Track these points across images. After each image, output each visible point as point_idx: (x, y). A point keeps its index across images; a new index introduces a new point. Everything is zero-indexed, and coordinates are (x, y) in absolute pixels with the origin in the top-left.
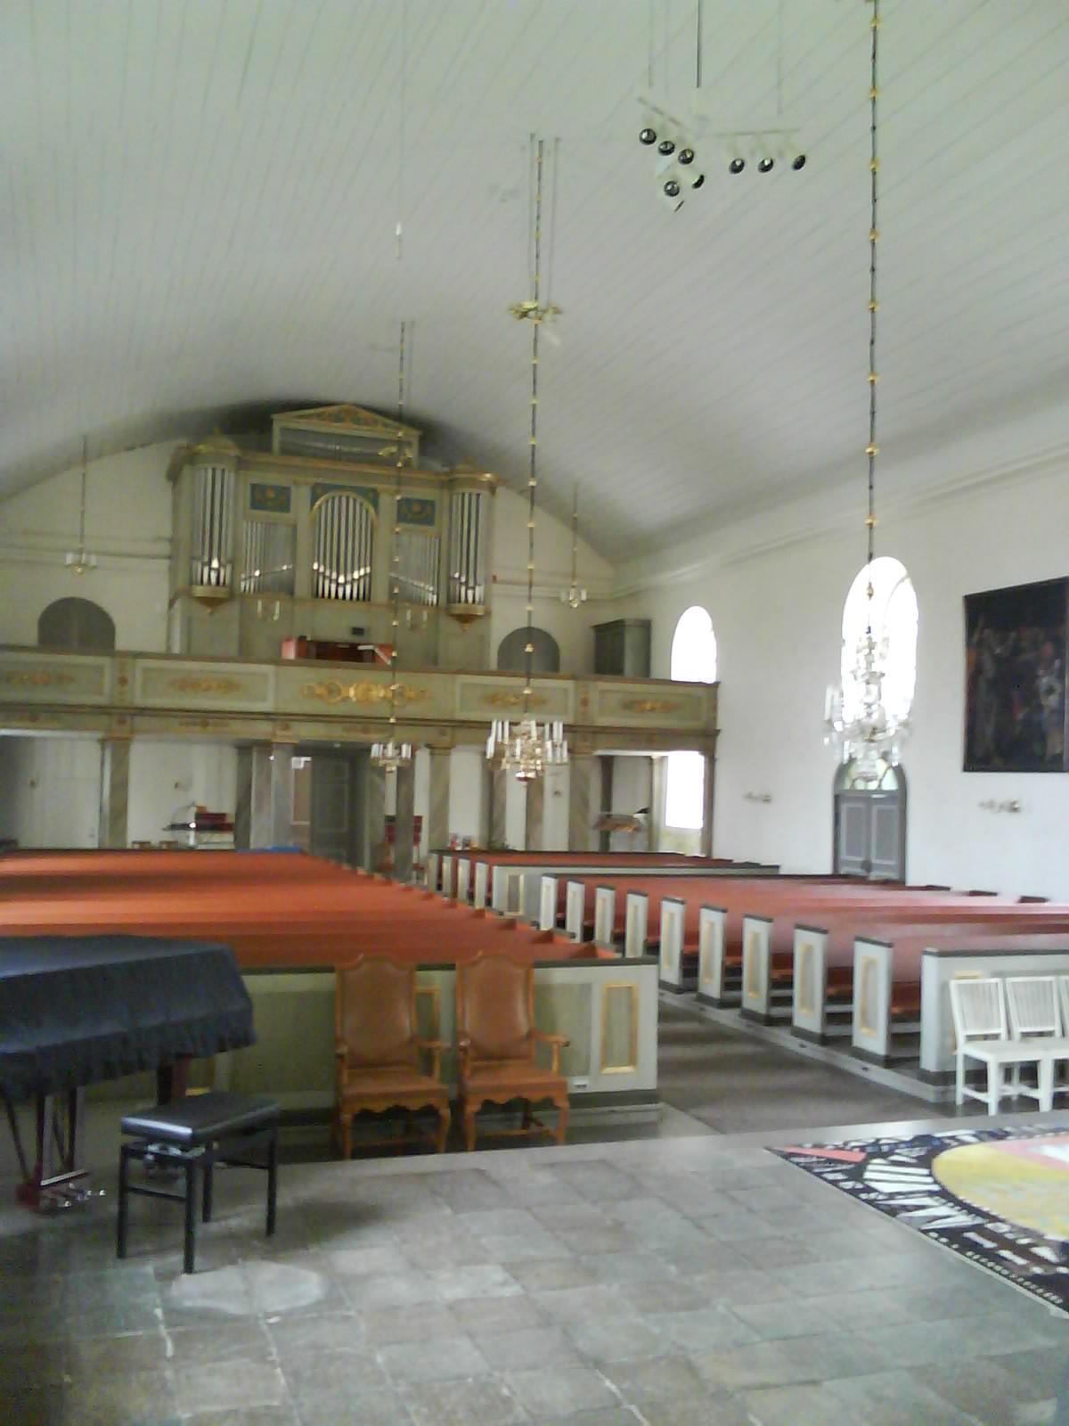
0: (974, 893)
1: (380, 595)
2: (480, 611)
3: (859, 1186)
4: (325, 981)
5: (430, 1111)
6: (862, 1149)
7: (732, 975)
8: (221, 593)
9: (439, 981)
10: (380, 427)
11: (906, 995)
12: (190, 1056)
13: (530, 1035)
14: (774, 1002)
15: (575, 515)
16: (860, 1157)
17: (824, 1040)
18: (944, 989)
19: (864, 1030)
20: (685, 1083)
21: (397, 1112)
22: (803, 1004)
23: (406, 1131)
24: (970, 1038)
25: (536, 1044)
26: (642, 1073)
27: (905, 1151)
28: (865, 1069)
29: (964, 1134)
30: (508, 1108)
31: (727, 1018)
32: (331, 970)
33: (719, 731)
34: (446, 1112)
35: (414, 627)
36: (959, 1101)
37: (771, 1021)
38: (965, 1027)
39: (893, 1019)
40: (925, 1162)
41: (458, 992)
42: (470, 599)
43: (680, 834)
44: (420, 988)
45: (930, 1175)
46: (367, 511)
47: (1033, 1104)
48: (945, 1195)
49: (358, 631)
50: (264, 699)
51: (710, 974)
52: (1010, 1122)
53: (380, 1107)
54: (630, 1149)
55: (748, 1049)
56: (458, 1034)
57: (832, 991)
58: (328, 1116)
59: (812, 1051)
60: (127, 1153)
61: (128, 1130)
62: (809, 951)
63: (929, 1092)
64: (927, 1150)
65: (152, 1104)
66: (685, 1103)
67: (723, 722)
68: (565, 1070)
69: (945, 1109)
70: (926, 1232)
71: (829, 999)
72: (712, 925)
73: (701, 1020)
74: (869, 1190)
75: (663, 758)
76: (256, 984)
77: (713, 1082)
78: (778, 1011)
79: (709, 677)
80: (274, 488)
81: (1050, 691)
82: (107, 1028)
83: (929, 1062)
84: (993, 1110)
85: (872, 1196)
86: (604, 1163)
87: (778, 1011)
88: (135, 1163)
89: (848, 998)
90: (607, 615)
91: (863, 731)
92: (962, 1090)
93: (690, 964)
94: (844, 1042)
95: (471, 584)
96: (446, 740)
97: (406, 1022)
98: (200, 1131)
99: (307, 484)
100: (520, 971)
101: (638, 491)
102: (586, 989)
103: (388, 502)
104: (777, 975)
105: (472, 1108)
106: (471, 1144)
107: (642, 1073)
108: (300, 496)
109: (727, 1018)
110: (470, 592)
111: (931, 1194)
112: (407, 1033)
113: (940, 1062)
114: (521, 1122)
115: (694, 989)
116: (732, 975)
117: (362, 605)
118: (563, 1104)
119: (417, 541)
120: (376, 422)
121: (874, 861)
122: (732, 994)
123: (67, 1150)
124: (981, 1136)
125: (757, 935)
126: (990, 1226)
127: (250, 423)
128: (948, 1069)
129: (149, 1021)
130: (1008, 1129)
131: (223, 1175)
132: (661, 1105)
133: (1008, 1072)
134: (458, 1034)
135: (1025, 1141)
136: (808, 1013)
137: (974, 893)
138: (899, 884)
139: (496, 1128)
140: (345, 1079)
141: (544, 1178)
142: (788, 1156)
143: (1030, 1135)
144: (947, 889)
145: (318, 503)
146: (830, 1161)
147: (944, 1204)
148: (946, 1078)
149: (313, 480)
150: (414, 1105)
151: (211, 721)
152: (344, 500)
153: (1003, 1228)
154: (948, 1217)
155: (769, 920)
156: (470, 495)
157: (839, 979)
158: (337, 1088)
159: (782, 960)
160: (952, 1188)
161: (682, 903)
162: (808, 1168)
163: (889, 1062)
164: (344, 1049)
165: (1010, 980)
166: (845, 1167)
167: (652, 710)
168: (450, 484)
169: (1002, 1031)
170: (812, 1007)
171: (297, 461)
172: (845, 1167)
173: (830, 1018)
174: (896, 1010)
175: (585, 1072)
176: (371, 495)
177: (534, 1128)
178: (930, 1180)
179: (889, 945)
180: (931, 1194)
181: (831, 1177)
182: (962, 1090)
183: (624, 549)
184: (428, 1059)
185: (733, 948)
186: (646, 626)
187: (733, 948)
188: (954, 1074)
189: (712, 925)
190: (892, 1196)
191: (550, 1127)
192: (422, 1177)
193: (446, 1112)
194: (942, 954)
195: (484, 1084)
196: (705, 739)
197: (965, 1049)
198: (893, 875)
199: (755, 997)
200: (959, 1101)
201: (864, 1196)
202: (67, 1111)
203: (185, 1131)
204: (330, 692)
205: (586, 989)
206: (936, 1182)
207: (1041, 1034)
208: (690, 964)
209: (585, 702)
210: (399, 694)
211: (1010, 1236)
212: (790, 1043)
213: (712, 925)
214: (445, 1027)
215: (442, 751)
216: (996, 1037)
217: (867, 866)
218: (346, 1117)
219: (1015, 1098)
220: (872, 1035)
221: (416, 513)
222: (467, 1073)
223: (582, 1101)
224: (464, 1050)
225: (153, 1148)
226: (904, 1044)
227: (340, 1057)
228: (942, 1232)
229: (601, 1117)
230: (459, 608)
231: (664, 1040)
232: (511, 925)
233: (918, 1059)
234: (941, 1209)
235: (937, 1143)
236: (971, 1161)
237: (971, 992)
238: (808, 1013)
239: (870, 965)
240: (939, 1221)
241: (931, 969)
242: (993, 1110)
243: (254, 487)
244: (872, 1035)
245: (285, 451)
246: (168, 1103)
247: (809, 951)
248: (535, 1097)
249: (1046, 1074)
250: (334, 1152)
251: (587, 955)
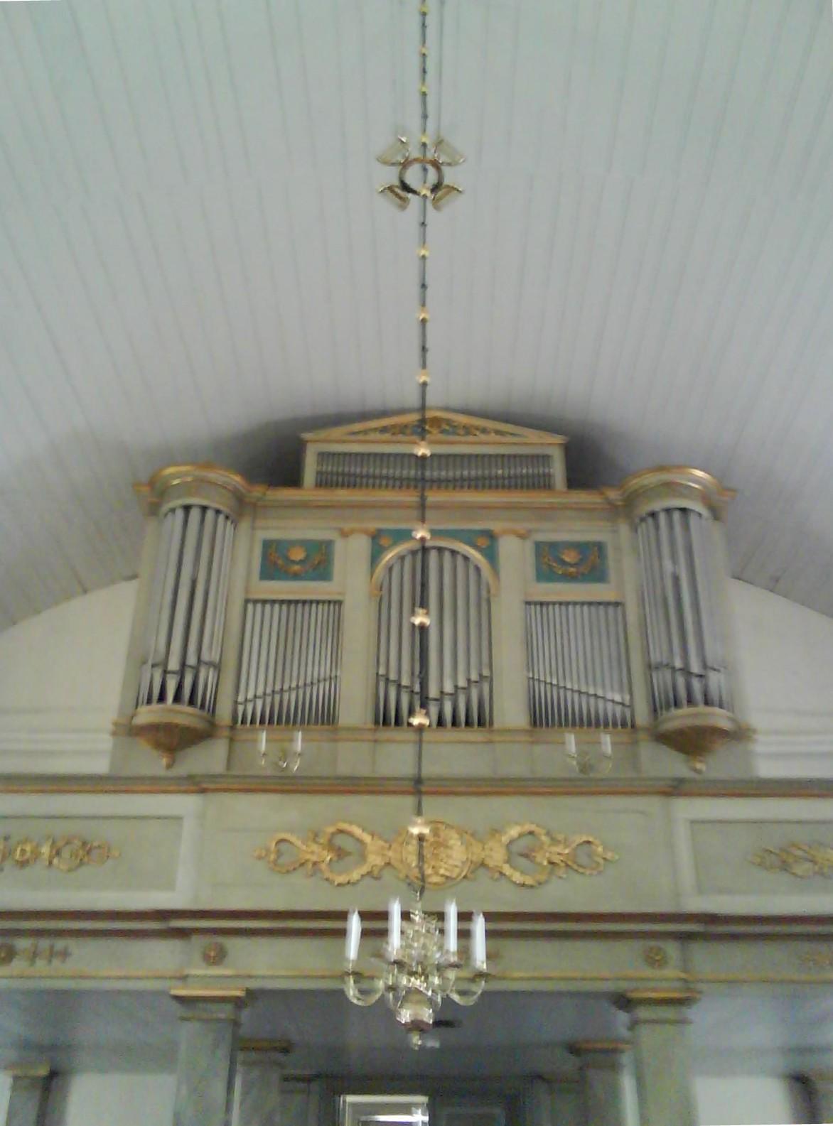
1: (511, 710)
8: (185, 716)
50: (170, 886)
80: (304, 543)
96: (666, 978)
99: (366, 532)
117: (475, 735)
120: (484, 431)
127: (275, 460)
145: (389, 556)
149: (373, 526)
151: (23, 944)
171: (342, 495)
204: (340, 853)
210: (522, 853)
215: (668, 1013)
230: (679, 718)
243: (267, 545)
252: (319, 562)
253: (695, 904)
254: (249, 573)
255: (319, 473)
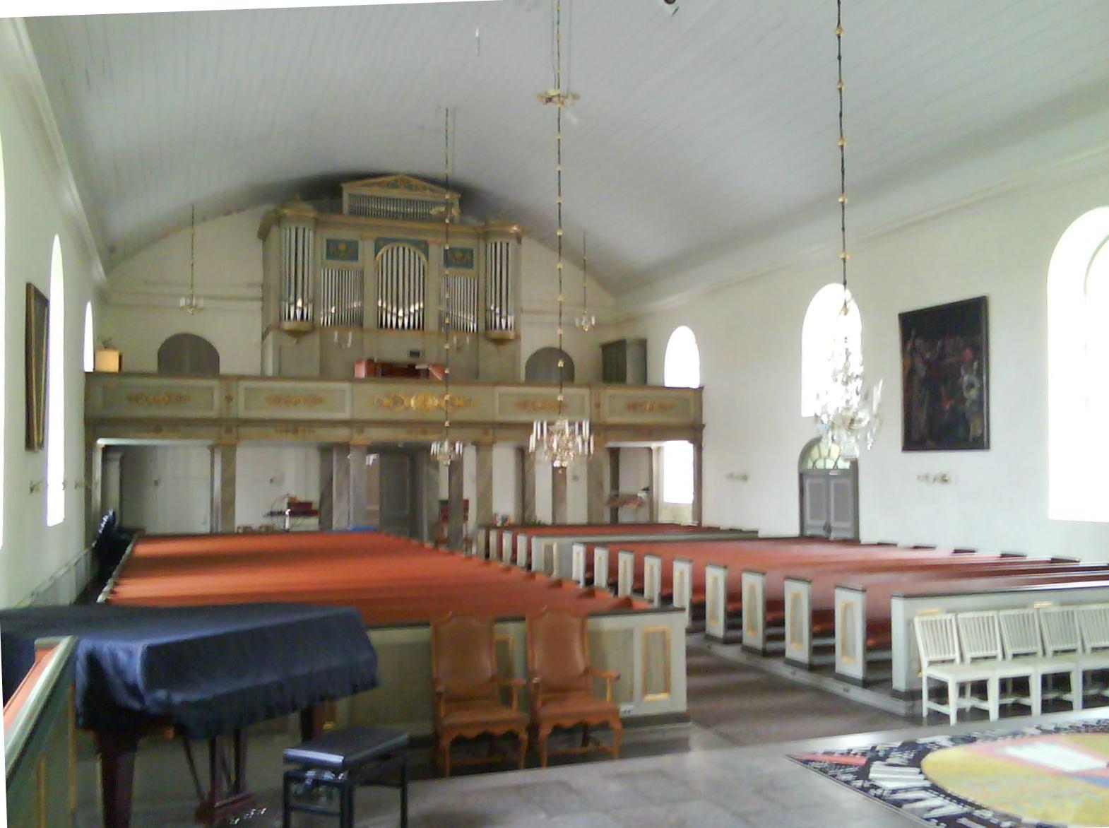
0: (916, 548)
1: (432, 323)
2: (511, 335)
3: (867, 784)
4: (422, 634)
5: (512, 736)
6: (864, 754)
7: (734, 617)
8: (305, 326)
9: (512, 632)
10: (428, 192)
11: (878, 630)
12: (334, 698)
13: (587, 671)
14: (769, 638)
15: (585, 258)
16: (863, 761)
17: (811, 668)
18: (909, 624)
19: (845, 659)
20: (706, 705)
21: (486, 738)
22: (793, 640)
23: (492, 753)
24: (931, 663)
25: (593, 678)
26: (674, 699)
27: (898, 754)
28: (847, 691)
29: (942, 739)
30: (570, 731)
31: (731, 653)
32: (427, 624)
33: (704, 426)
34: (524, 736)
35: (459, 349)
36: (925, 713)
37: (766, 654)
38: (927, 654)
39: (868, 649)
40: (916, 762)
41: (529, 640)
42: (504, 326)
43: (676, 508)
44: (498, 637)
45: (921, 773)
46: (419, 259)
47: (984, 714)
48: (936, 789)
49: (415, 354)
51: (714, 617)
52: (973, 728)
53: (472, 733)
54: (666, 761)
55: (751, 677)
56: (529, 674)
57: (817, 628)
58: (431, 742)
59: (802, 677)
60: (289, 778)
61: (289, 760)
62: (796, 598)
63: (900, 707)
64: (917, 755)
65: (299, 740)
66: (706, 722)
67: (707, 418)
68: (616, 699)
69: (914, 719)
70: (928, 820)
71: (814, 635)
72: (716, 580)
73: (708, 654)
74: (876, 787)
75: (659, 449)
76: (375, 636)
77: (732, 704)
78: (773, 646)
79: (695, 385)
81: (971, 386)
82: (267, 678)
83: (899, 682)
84: (953, 720)
85: (879, 792)
86: (660, 773)
87: (773, 646)
88: (294, 787)
89: (831, 633)
90: (611, 336)
91: (844, 422)
92: (927, 705)
93: (698, 611)
94: (829, 669)
95: (504, 313)
96: (488, 438)
97: (487, 664)
98: (352, 758)
100: (576, 622)
101: (634, 236)
102: (629, 633)
103: (436, 252)
104: (770, 616)
105: (545, 731)
106: (545, 759)
107: (674, 699)
108: (366, 248)
109: (731, 653)
110: (503, 321)
111: (925, 789)
112: (489, 674)
113: (908, 683)
114: (583, 742)
115: (703, 629)
116: (734, 617)
117: (418, 334)
118: (618, 726)
119: (461, 280)
120: (425, 189)
121: (833, 524)
122: (733, 634)
123: (233, 777)
124: (956, 741)
125: (753, 587)
126: (977, 813)
127: (324, 191)
128: (916, 687)
129: (300, 670)
130: (975, 734)
131: (363, 794)
132: (690, 724)
133: (962, 689)
134: (529, 674)
135: (988, 744)
136: (798, 647)
137: (916, 548)
138: (854, 541)
139: (562, 748)
140: (443, 712)
141: (615, 787)
142: (806, 762)
143: (994, 739)
144: (895, 545)
146: (839, 765)
147: (939, 796)
148: (914, 695)
149: (376, 235)
150: (499, 731)
152: (401, 250)
153: (988, 815)
154: (941, 807)
155: (764, 574)
156: (501, 244)
157: (823, 620)
158: (435, 718)
159: (774, 606)
160: (942, 783)
161: (691, 561)
162: (823, 771)
163: (866, 684)
164: (440, 688)
165: (960, 616)
166: (852, 769)
167: (652, 409)
168: (484, 235)
169: (957, 656)
170: (801, 641)
171: (363, 220)
172: (852, 769)
173: (816, 650)
174: (871, 642)
175: (630, 699)
176: (423, 246)
177: (591, 746)
178: (922, 777)
179: (864, 591)
180: (925, 789)
181: (844, 777)
182: (927, 705)
183: (622, 283)
184: (506, 696)
185: (734, 596)
186: (643, 344)
187: (734, 596)
188: (921, 691)
189: (716, 579)
190: (894, 791)
191: (605, 744)
192: (518, 789)
193: (524, 736)
194: (907, 596)
195: (552, 712)
196: (694, 432)
197: (927, 672)
198: (849, 535)
199: (753, 635)
200: (925, 713)
201: (872, 792)
202: (233, 743)
203: (336, 759)
205: (629, 633)
206: (926, 779)
207: (986, 658)
208: (698, 611)
209: (598, 405)
211: (995, 821)
212: (785, 672)
213: (716, 579)
214: (518, 668)
216: (952, 661)
217: (828, 528)
218: (446, 742)
219: (968, 710)
220: (851, 663)
221: (458, 259)
222: (539, 704)
223: (631, 723)
224: (537, 685)
225: (311, 774)
226: (878, 670)
227: (439, 695)
228: (940, 819)
229: (647, 737)
230: (495, 334)
231: (691, 671)
232: (558, 584)
233: (890, 680)
234: (938, 801)
235: (920, 748)
236: (947, 759)
237: (931, 626)
238: (798, 647)
239: (848, 607)
240: (935, 810)
241: (899, 611)
242: (953, 720)
243: (329, 242)
244: (851, 663)
245: (355, 212)
246: (310, 737)
247: (796, 598)
248: (595, 721)
249: (993, 690)
250: (434, 772)
251: (625, 607)
252: (351, 252)
253: (500, 418)
254: (322, 257)
255: (350, 206)
